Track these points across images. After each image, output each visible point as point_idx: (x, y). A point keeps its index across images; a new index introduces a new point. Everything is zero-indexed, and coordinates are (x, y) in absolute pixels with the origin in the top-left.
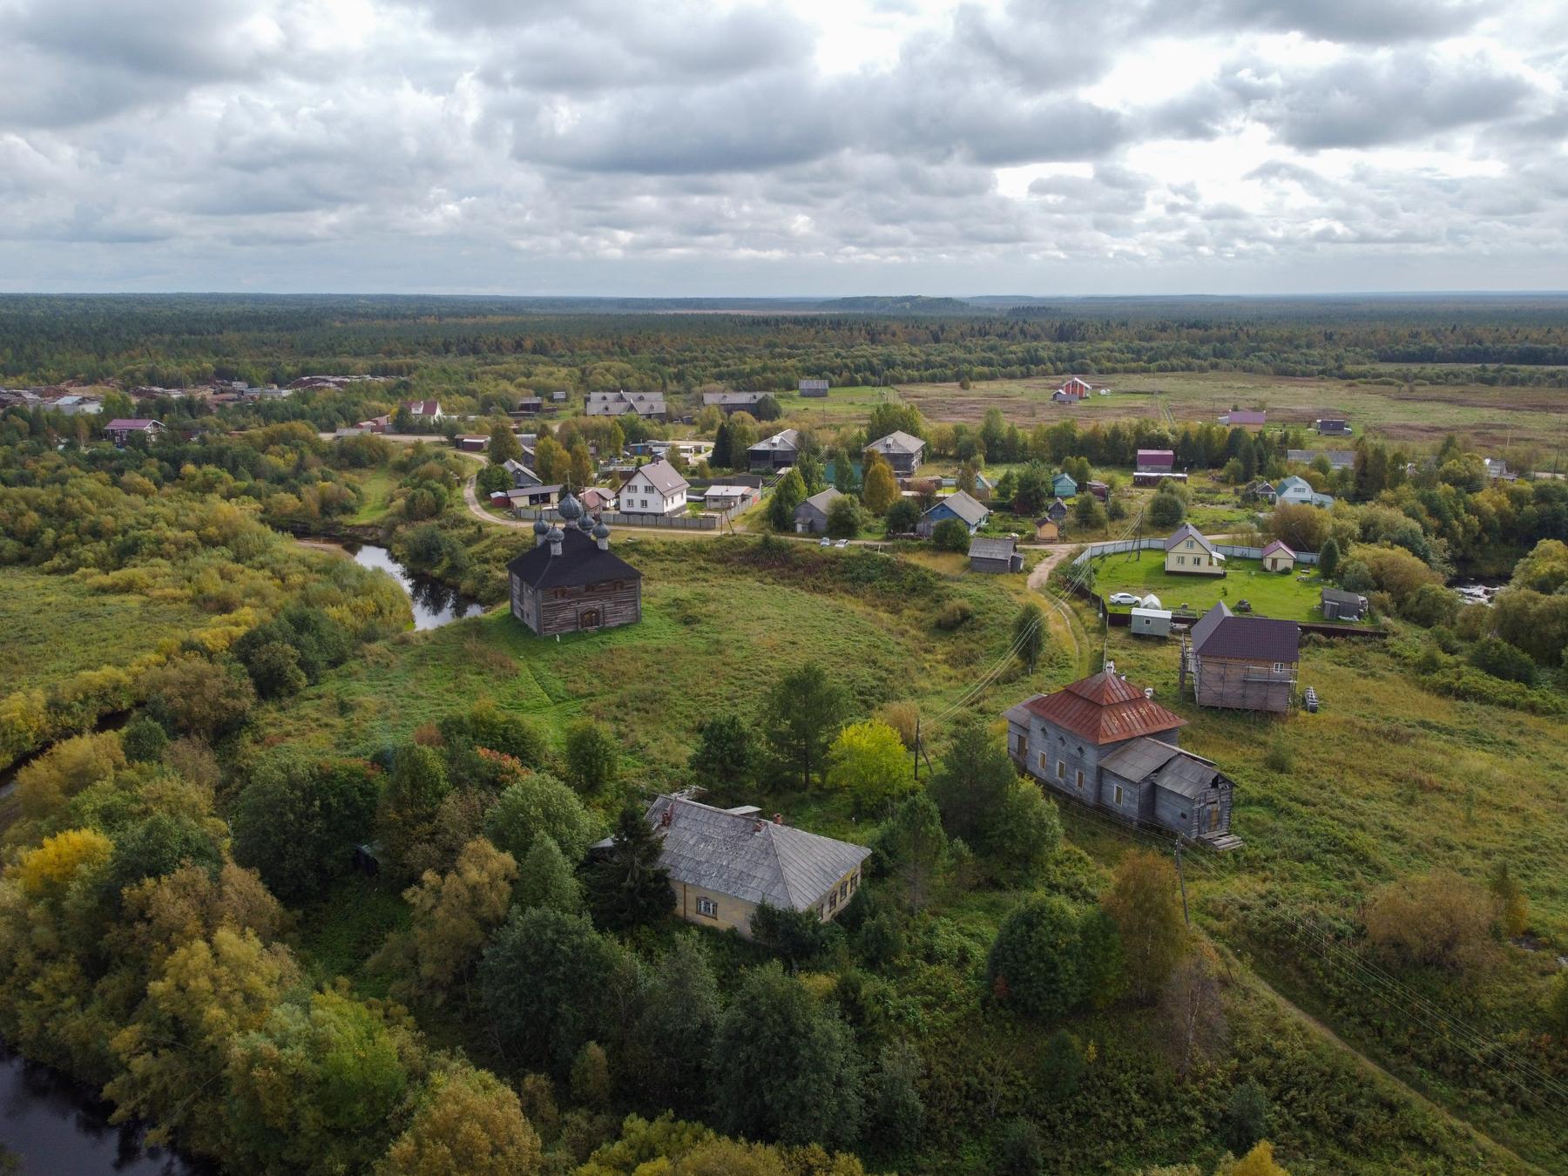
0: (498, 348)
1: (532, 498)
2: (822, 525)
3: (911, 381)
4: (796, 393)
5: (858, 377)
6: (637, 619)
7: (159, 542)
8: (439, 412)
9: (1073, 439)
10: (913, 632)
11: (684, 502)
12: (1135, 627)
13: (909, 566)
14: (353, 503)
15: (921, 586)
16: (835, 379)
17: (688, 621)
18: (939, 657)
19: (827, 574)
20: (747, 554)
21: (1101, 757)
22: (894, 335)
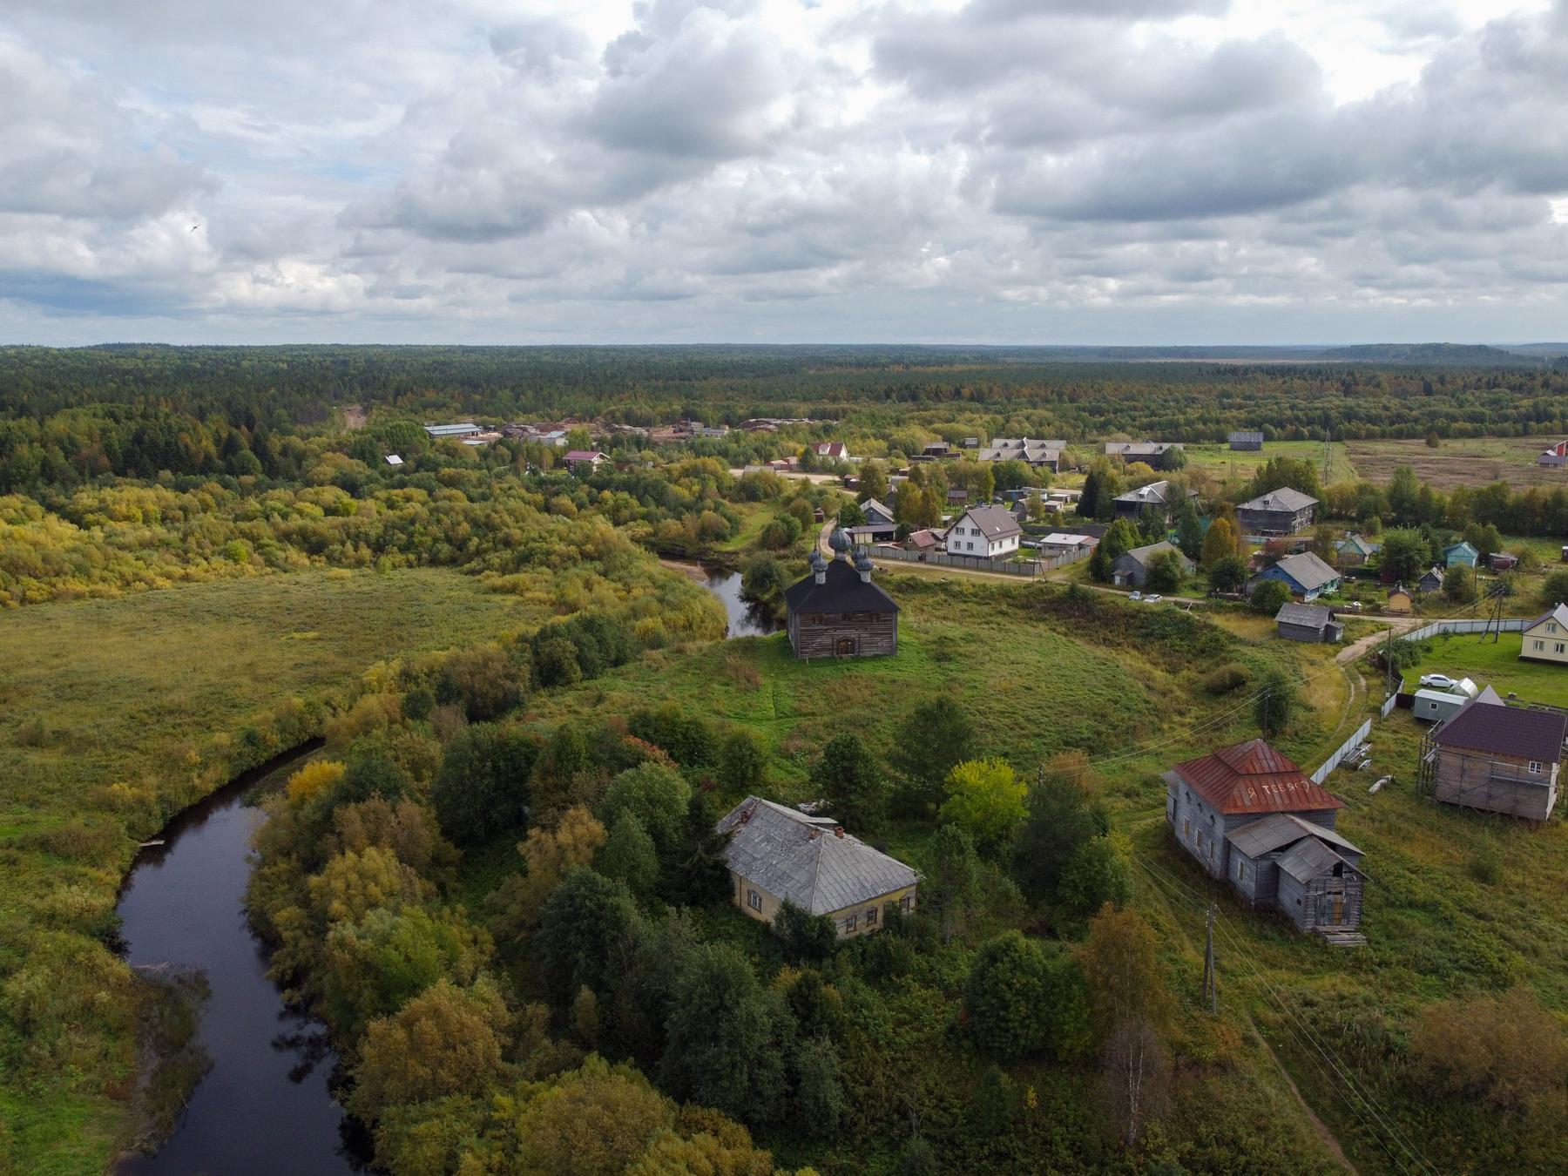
0: (937, 396)
1: (875, 535)
2: (1142, 578)
3: (1371, 436)
4: (1226, 446)
5: (1305, 431)
6: (892, 650)
7: (548, 553)
8: (843, 454)
9: (1502, 505)
10: (1178, 693)
11: (1016, 546)
12: (1418, 711)
13: (1206, 626)
14: (727, 532)
15: (1214, 647)
16: (1275, 432)
17: (941, 658)
18: (1188, 720)
19: (1123, 629)
20: (1050, 602)
21: (1228, 829)
22: (1378, 385)
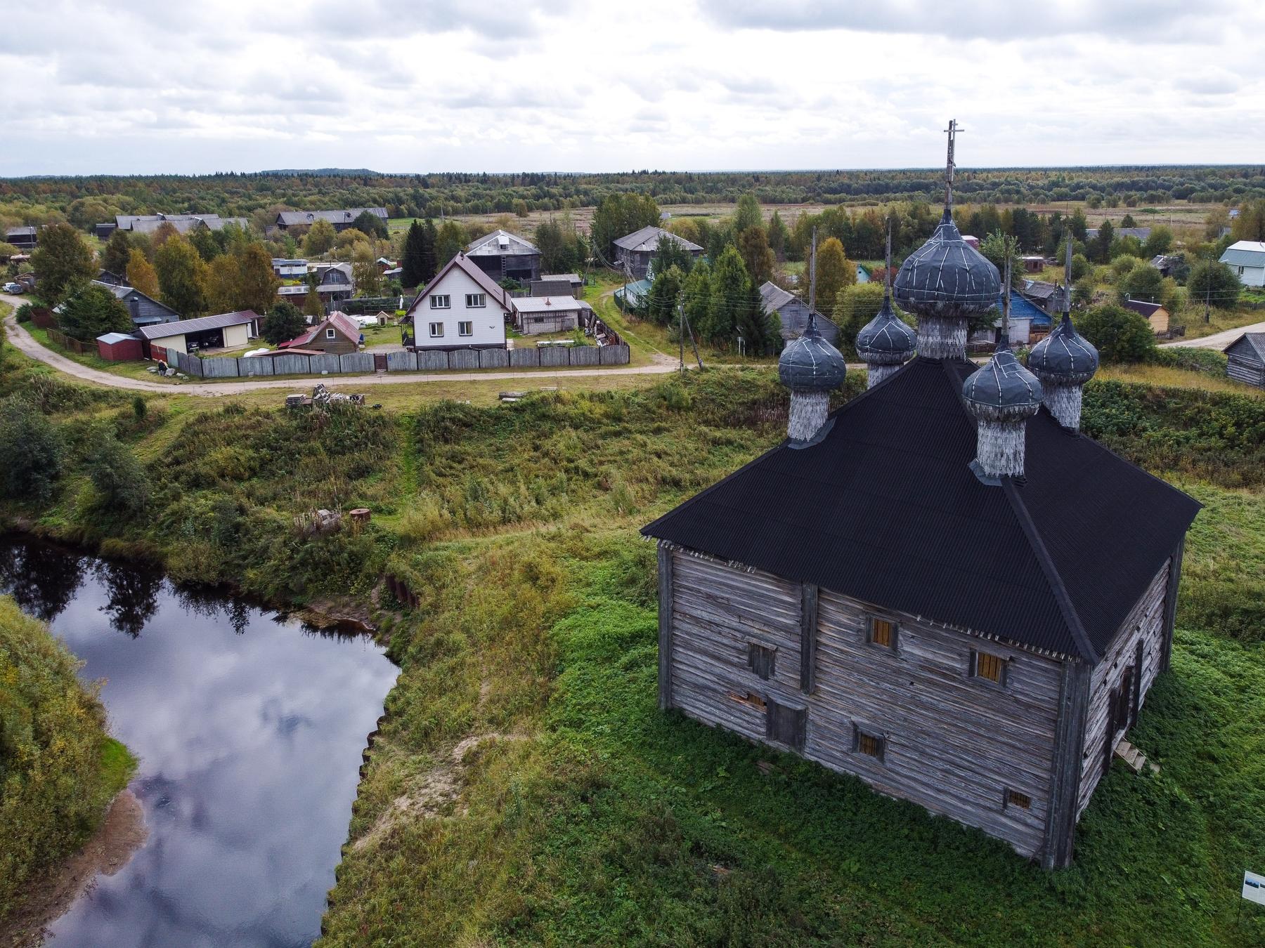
1: (190, 338)
